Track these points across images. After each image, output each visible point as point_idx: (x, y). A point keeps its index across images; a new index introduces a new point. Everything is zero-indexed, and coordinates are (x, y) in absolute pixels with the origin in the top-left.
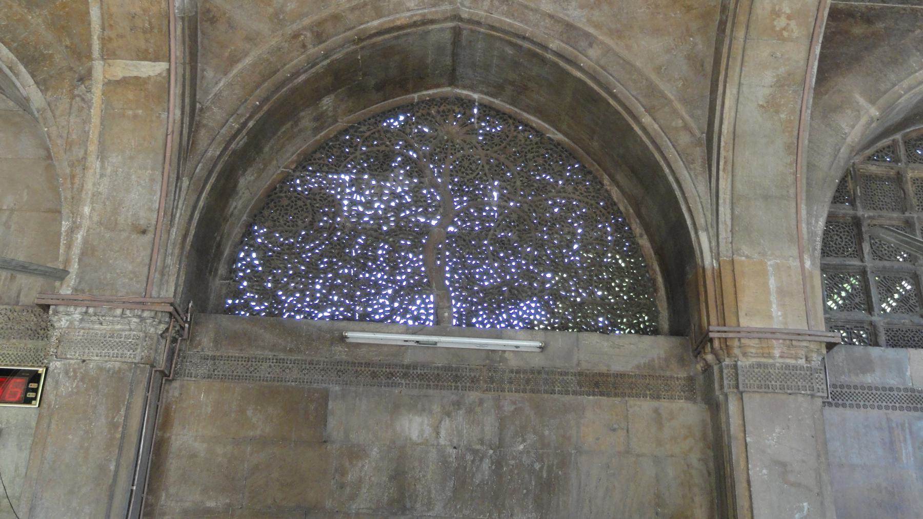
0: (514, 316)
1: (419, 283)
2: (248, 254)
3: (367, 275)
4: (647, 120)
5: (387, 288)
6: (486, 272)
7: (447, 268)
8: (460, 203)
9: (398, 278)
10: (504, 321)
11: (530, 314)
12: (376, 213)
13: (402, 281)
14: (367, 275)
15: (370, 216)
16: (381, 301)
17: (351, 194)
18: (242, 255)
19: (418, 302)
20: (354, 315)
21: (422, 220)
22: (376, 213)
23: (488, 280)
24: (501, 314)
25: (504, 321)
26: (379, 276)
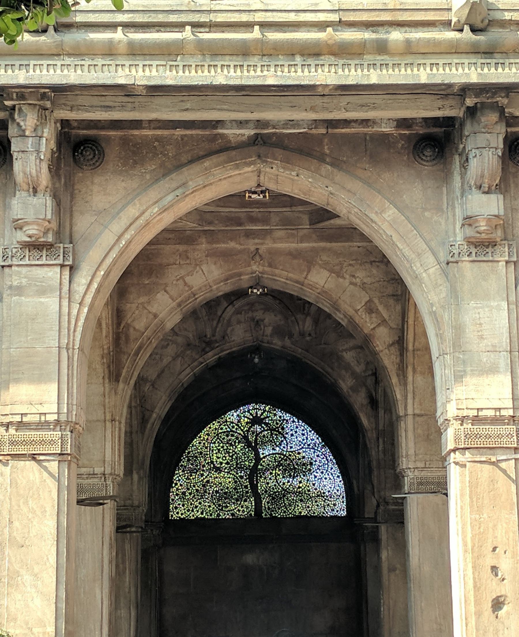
0: (287, 504)
1: (247, 492)
2: (176, 484)
3: (226, 490)
4: (334, 432)
5: (235, 495)
6: (275, 485)
7: (259, 485)
8: (263, 454)
9: (239, 490)
10: (283, 506)
11: (293, 503)
12: (228, 462)
13: (241, 492)
14: (226, 490)
15: (226, 464)
16: (233, 501)
17: (216, 453)
18: (174, 485)
19: (248, 500)
20: (222, 508)
21: (247, 463)
22: (228, 462)
23: (276, 488)
24: (282, 503)
25: (283, 506)
26: (231, 490)
